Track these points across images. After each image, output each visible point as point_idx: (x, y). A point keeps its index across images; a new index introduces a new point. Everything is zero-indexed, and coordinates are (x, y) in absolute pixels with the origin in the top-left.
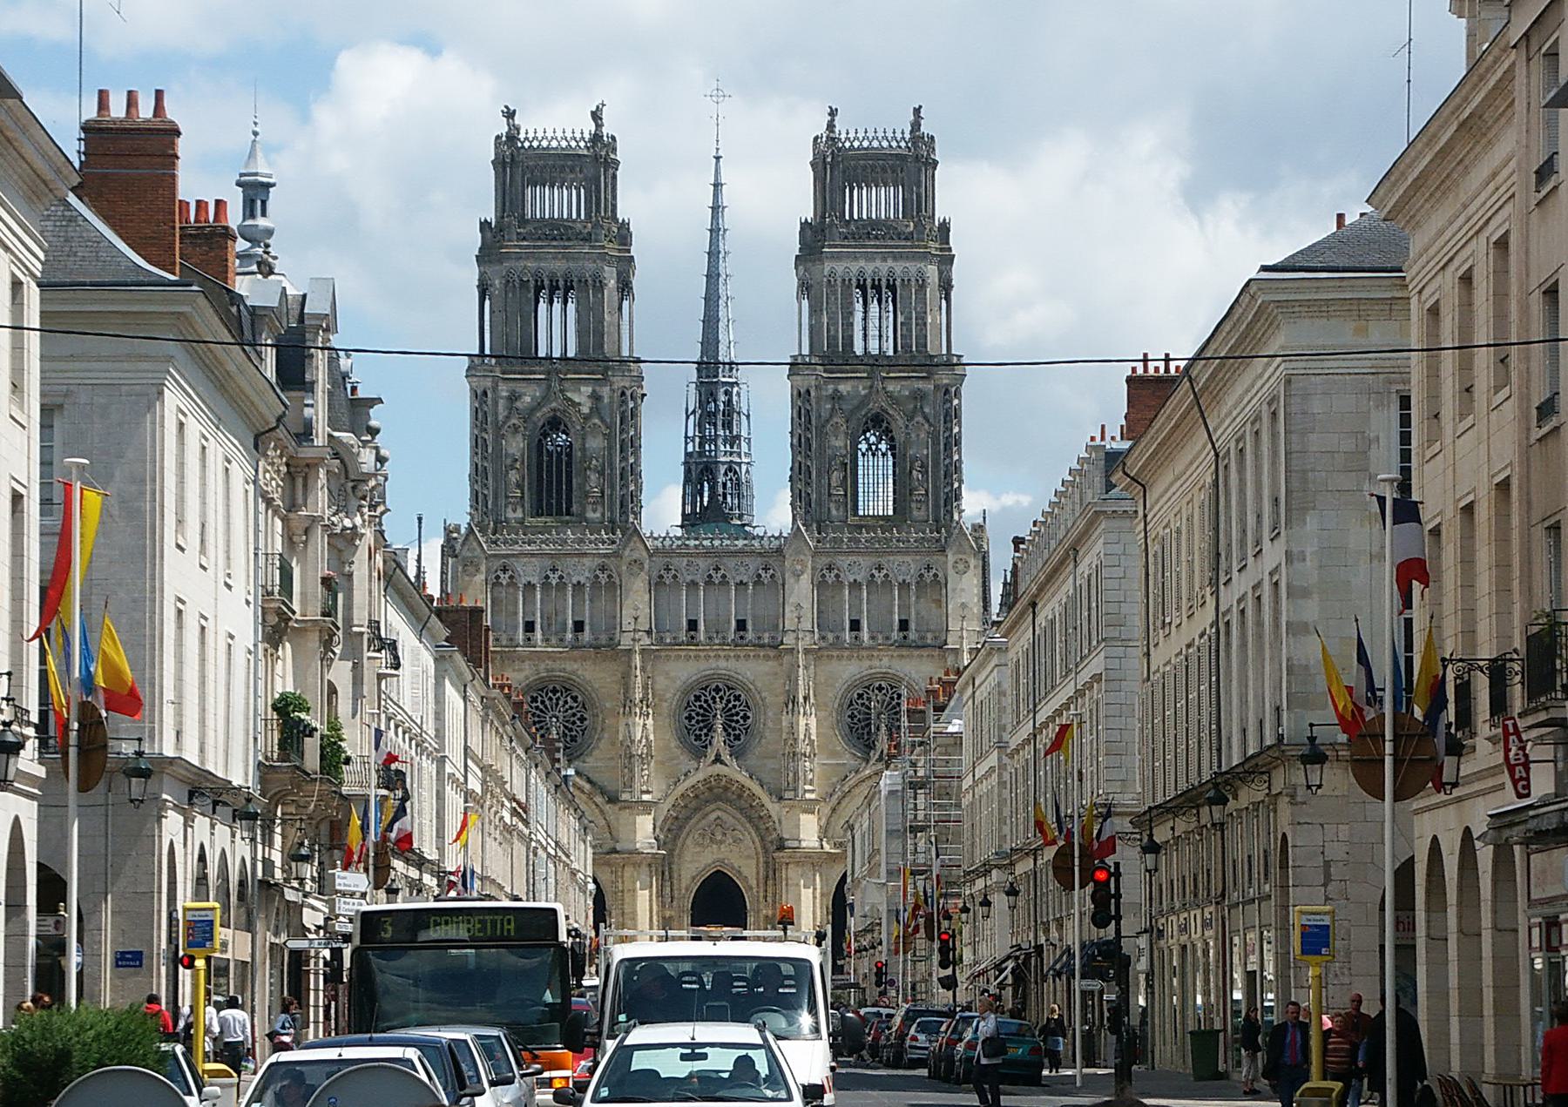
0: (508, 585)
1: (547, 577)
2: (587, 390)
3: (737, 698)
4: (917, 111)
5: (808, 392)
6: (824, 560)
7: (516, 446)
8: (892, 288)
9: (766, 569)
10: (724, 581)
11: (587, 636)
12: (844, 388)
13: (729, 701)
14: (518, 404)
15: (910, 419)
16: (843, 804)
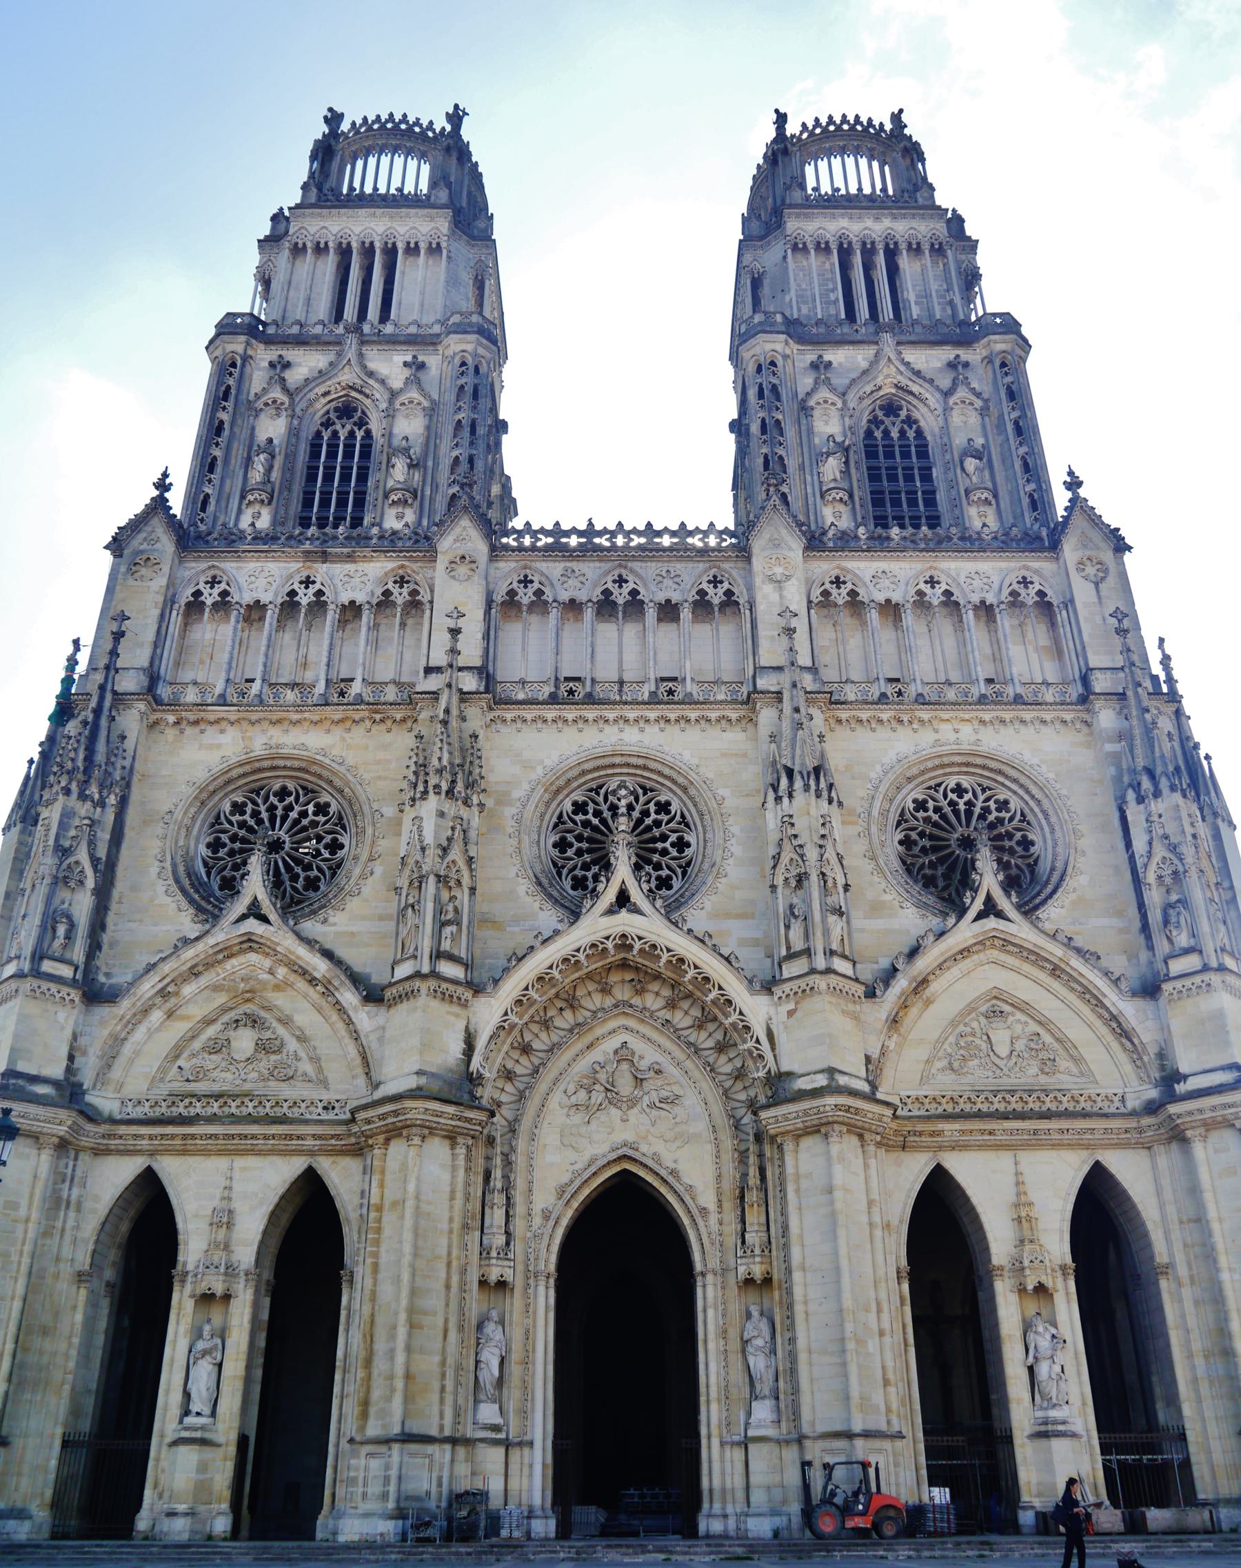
0: (215, 604)
1: (292, 593)
2: (401, 357)
3: (663, 807)
4: (897, 118)
5: (773, 364)
6: (824, 567)
7: (272, 428)
8: (891, 254)
9: (715, 582)
10: (635, 605)
11: (356, 688)
12: (836, 356)
13: (646, 813)
14: (287, 374)
15: (947, 394)
16: (914, 1011)
